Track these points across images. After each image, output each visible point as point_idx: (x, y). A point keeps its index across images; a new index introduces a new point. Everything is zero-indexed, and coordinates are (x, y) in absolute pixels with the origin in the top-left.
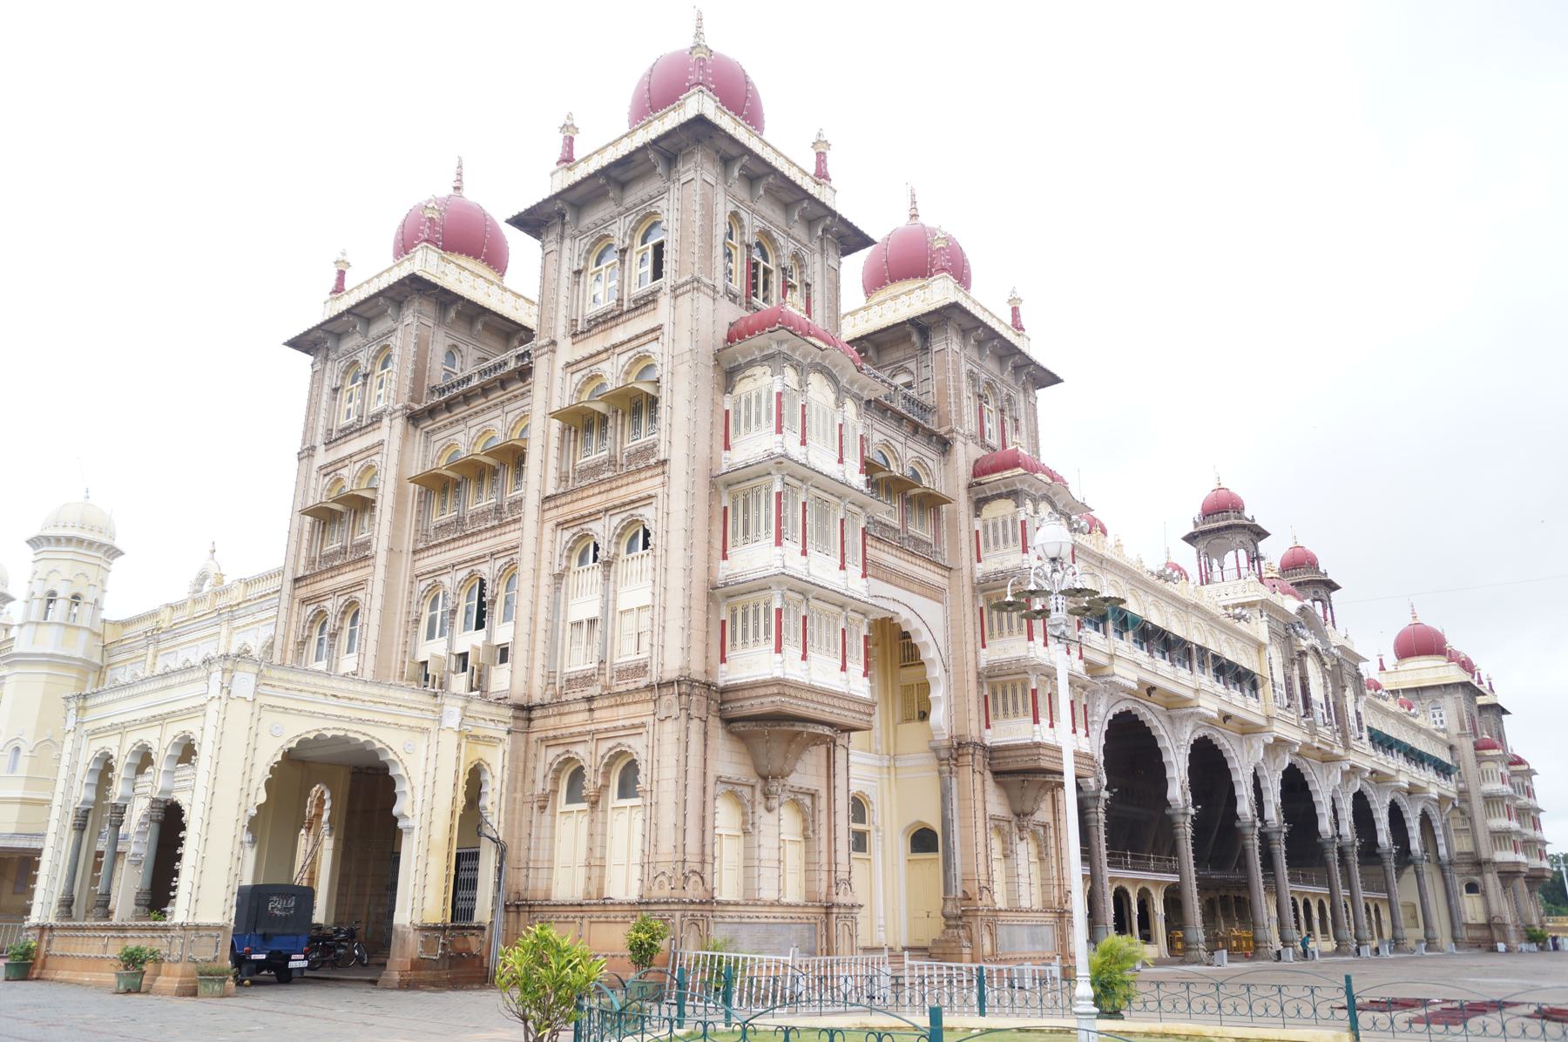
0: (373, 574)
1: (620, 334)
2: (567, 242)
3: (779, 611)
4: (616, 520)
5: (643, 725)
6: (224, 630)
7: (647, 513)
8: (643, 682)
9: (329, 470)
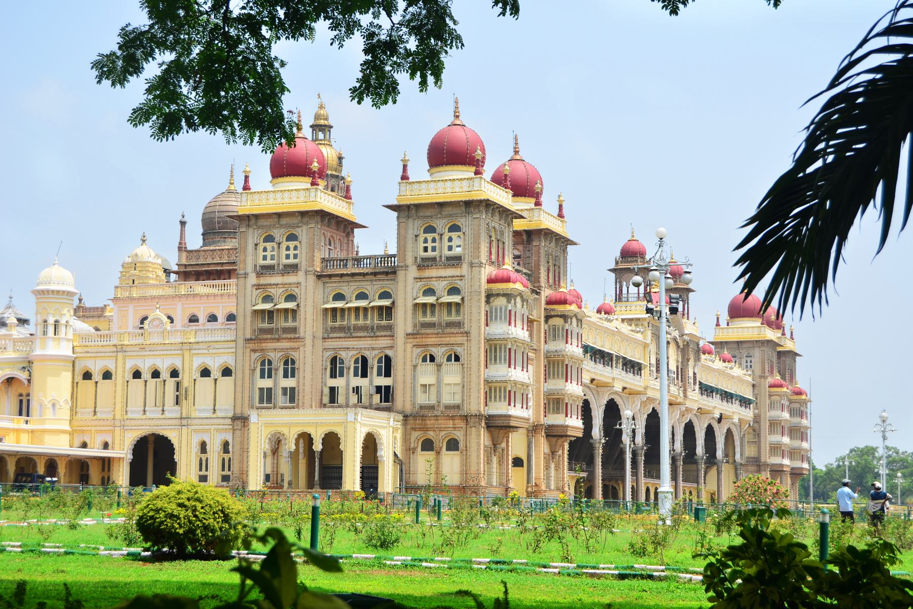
2: (411, 220)
3: (510, 392)
6: (187, 354)
7: (459, 350)
9: (258, 287)
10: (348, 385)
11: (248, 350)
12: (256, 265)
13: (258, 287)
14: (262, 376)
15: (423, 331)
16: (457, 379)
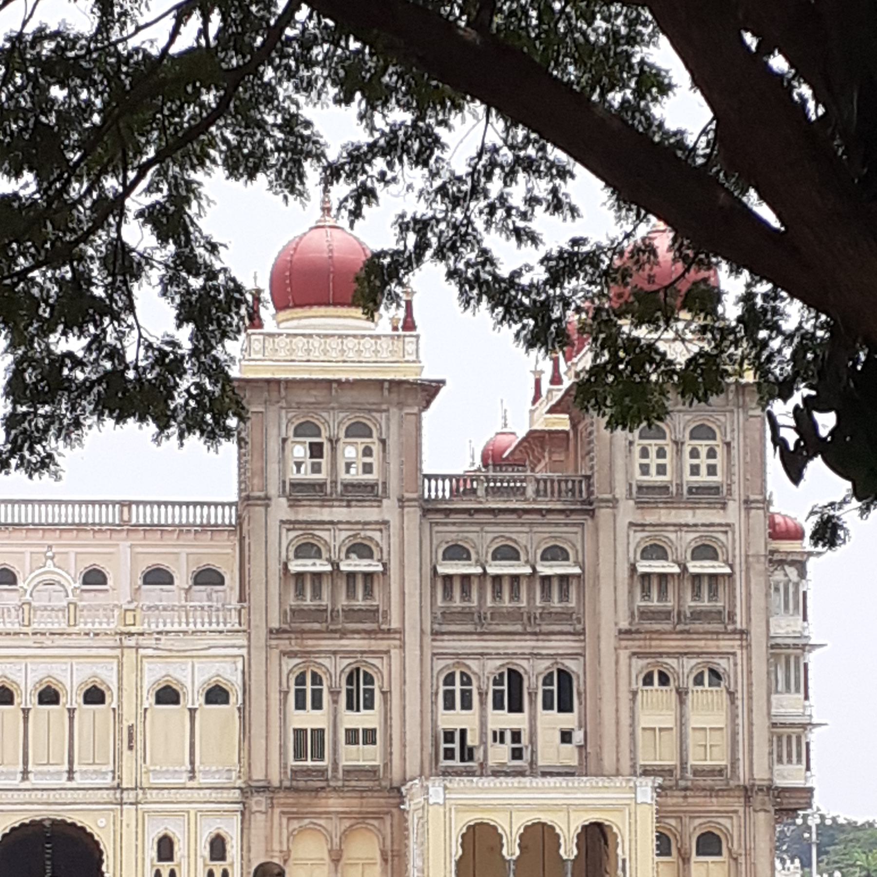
0: (402, 647)
1: (687, 517)
4: (693, 662)
5: (736, 812)
7: (723, 664)
8: (732, 783)
9: (291, 524)
10: (483, 724)
11: (276, 652)
12: (284, 482)
13: (291, 524)
14: (300, 705)
15: (647, 626)
16: (719, 719)
